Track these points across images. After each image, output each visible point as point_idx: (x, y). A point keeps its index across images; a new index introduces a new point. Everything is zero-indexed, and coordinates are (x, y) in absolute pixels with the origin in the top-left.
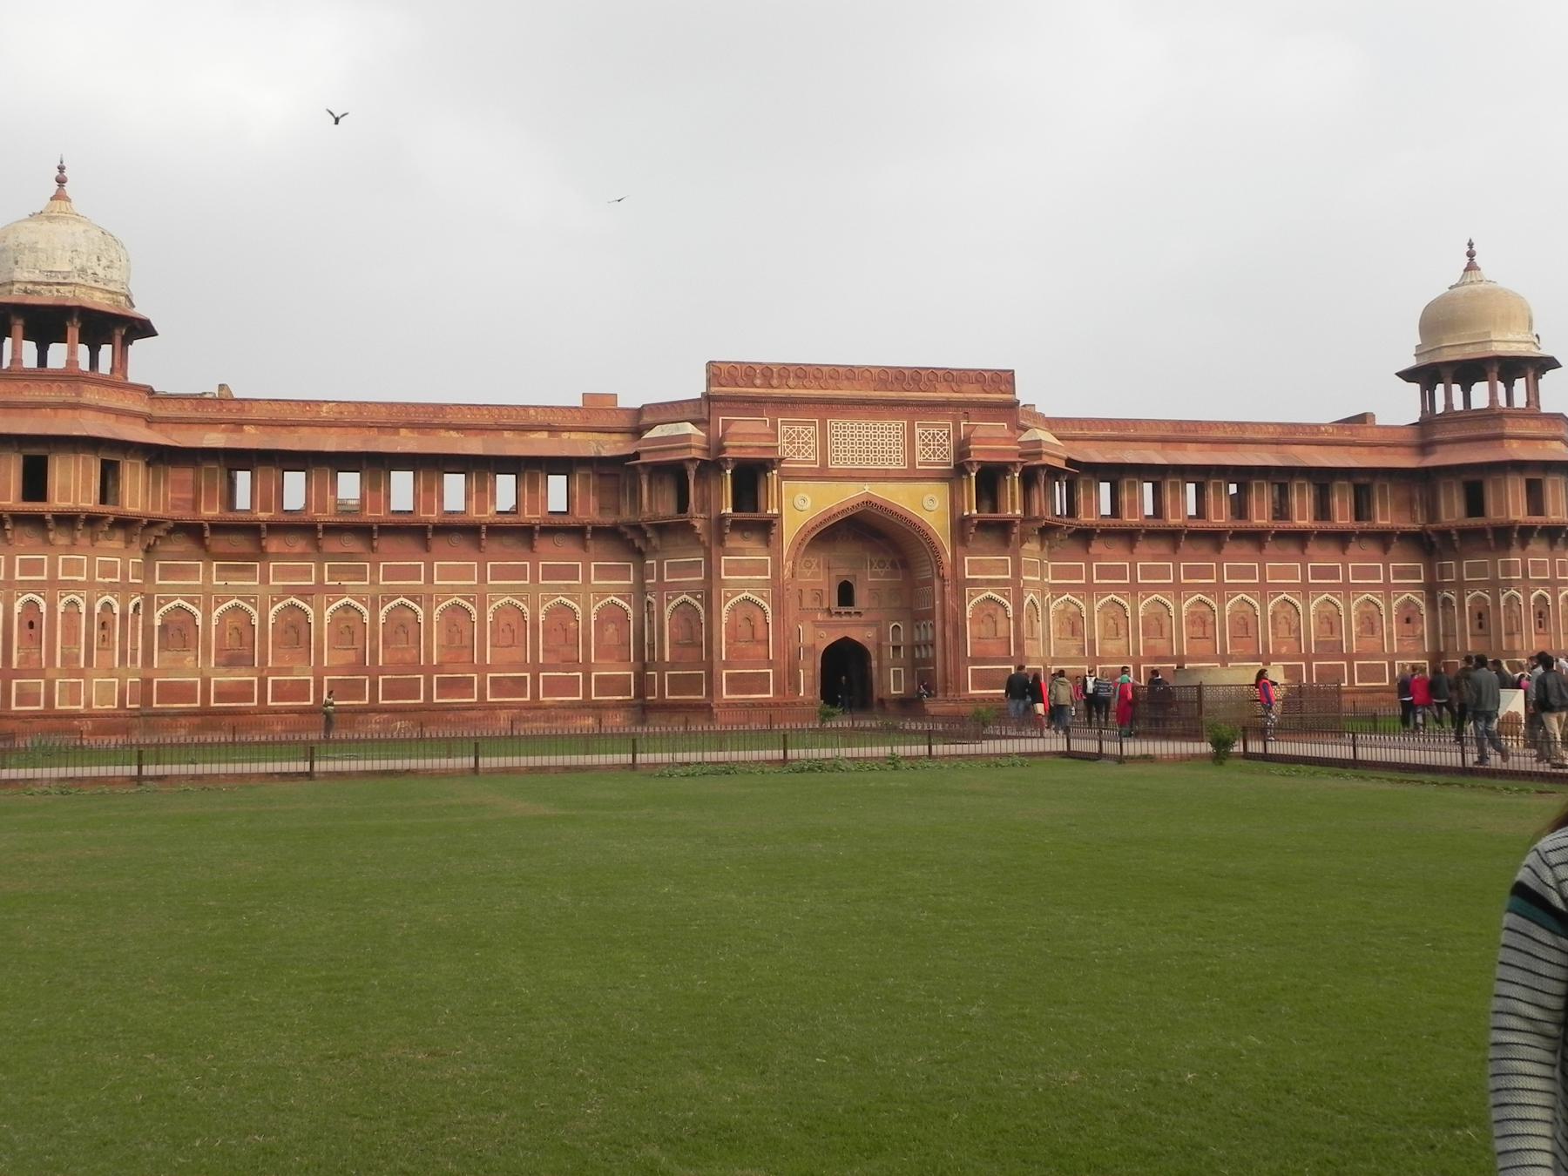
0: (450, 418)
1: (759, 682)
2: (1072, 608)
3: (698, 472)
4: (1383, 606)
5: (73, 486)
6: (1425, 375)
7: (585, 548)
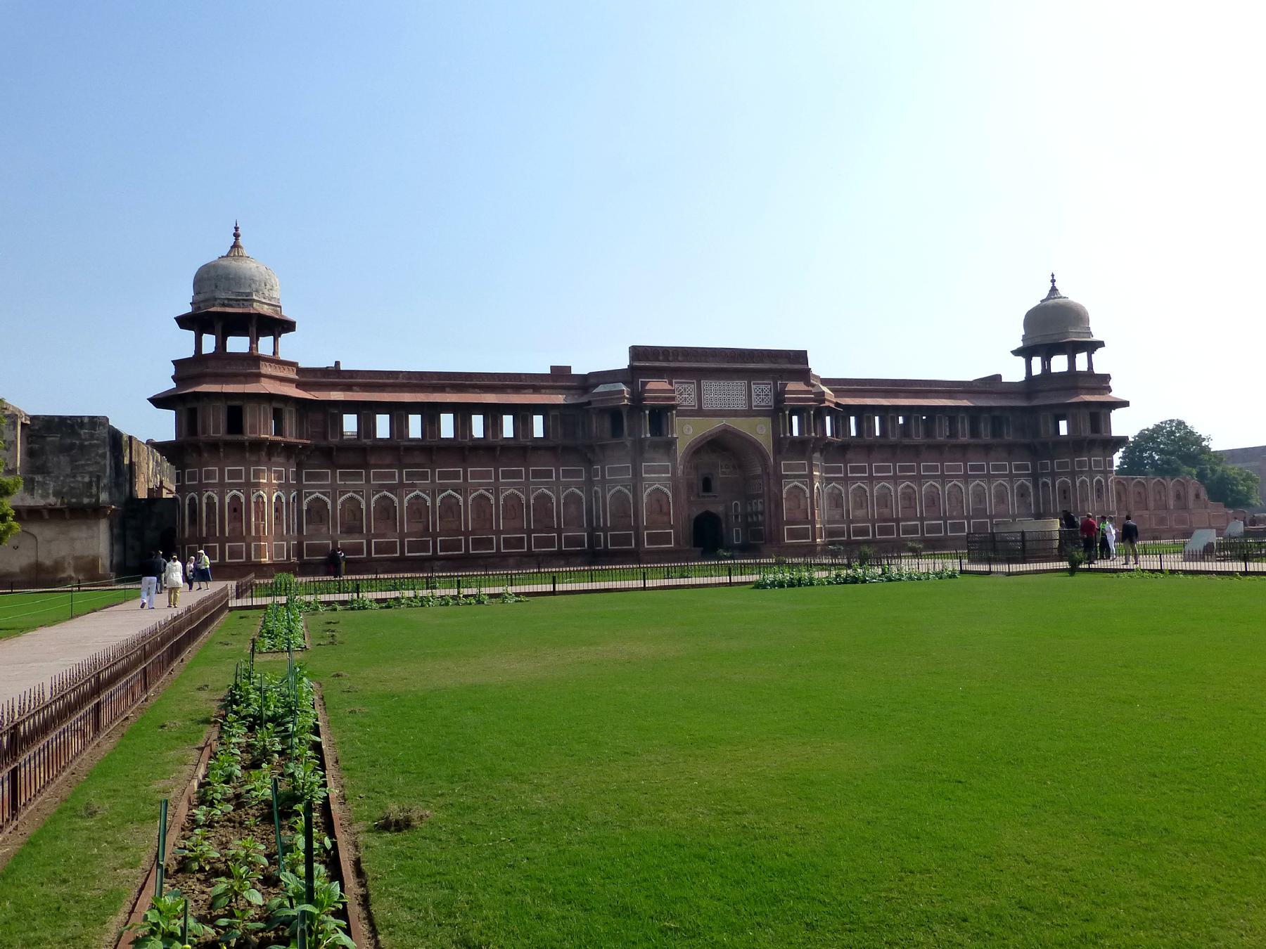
6: (1026, 352)
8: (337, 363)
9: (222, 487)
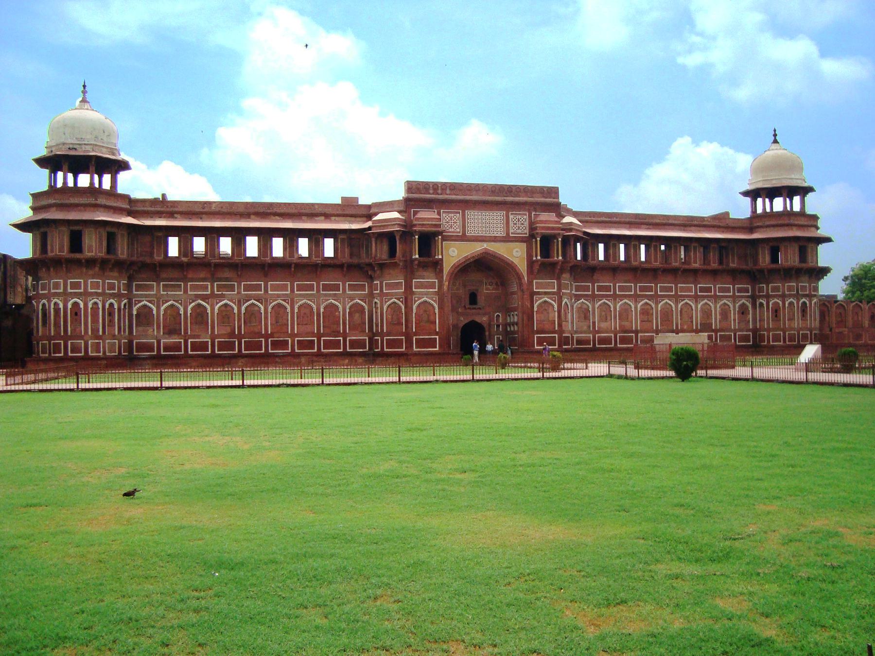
0: (275, 210)
1: (432, 343)
2: (585, 306)
3: (401, 236)
4: (731, 306)
5: (93, 245)
7: (345, 276)
8: (164, 195)
9: (66, 295)
